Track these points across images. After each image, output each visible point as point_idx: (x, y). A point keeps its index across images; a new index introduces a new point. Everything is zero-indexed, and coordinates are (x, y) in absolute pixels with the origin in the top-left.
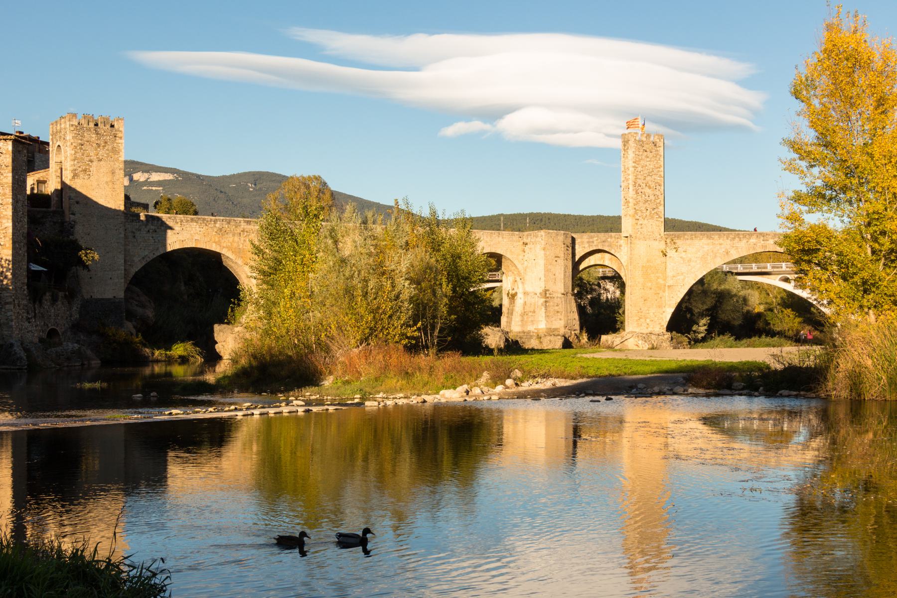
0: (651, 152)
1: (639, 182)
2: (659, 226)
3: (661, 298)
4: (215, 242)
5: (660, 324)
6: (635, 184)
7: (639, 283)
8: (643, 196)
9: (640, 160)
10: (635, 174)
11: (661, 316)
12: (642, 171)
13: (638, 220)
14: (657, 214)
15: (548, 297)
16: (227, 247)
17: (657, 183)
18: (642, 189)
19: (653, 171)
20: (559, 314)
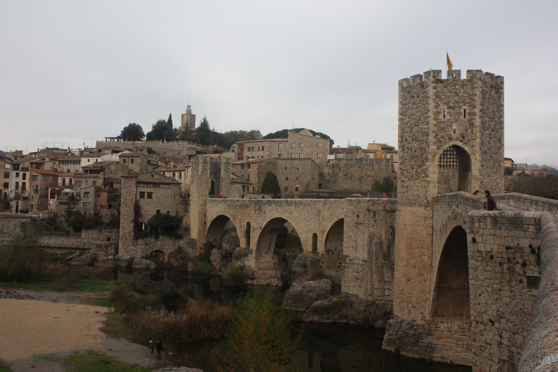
0: (418, 97)
1: (406, 136)
2: (425, 187)
3: (425, 280)
4: (228, 212)
5: (422, 313)
6: (402, 139)
7: (403, 257)
8: (410, 152)
9: (407, 109)
10: (402, 128)
11: (424, 304)
12: (409, 122)
13: (403, 181)
14: (424, 172)
15: (347, 263)
16: (231, 215)
17: (424, 132)
18: (408, 143)
19: (420, 119)
20: (358, 281)
